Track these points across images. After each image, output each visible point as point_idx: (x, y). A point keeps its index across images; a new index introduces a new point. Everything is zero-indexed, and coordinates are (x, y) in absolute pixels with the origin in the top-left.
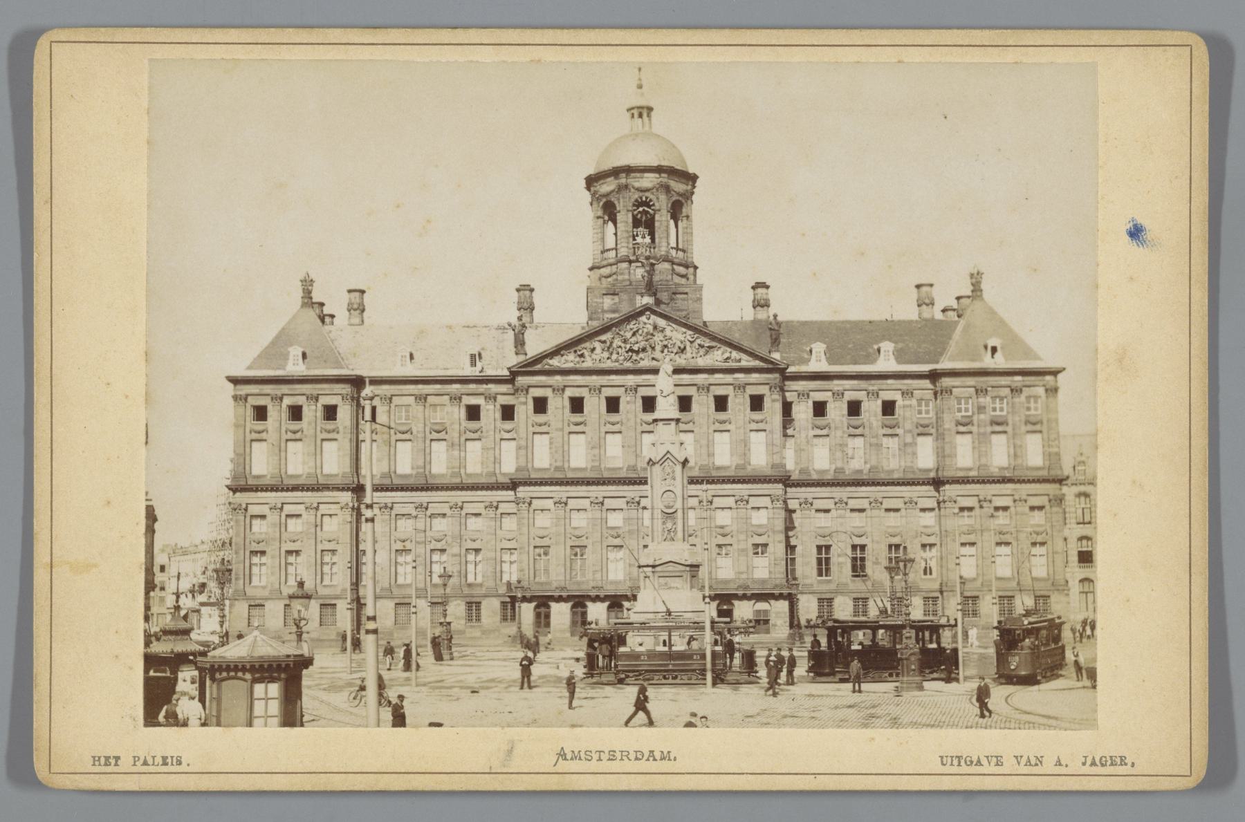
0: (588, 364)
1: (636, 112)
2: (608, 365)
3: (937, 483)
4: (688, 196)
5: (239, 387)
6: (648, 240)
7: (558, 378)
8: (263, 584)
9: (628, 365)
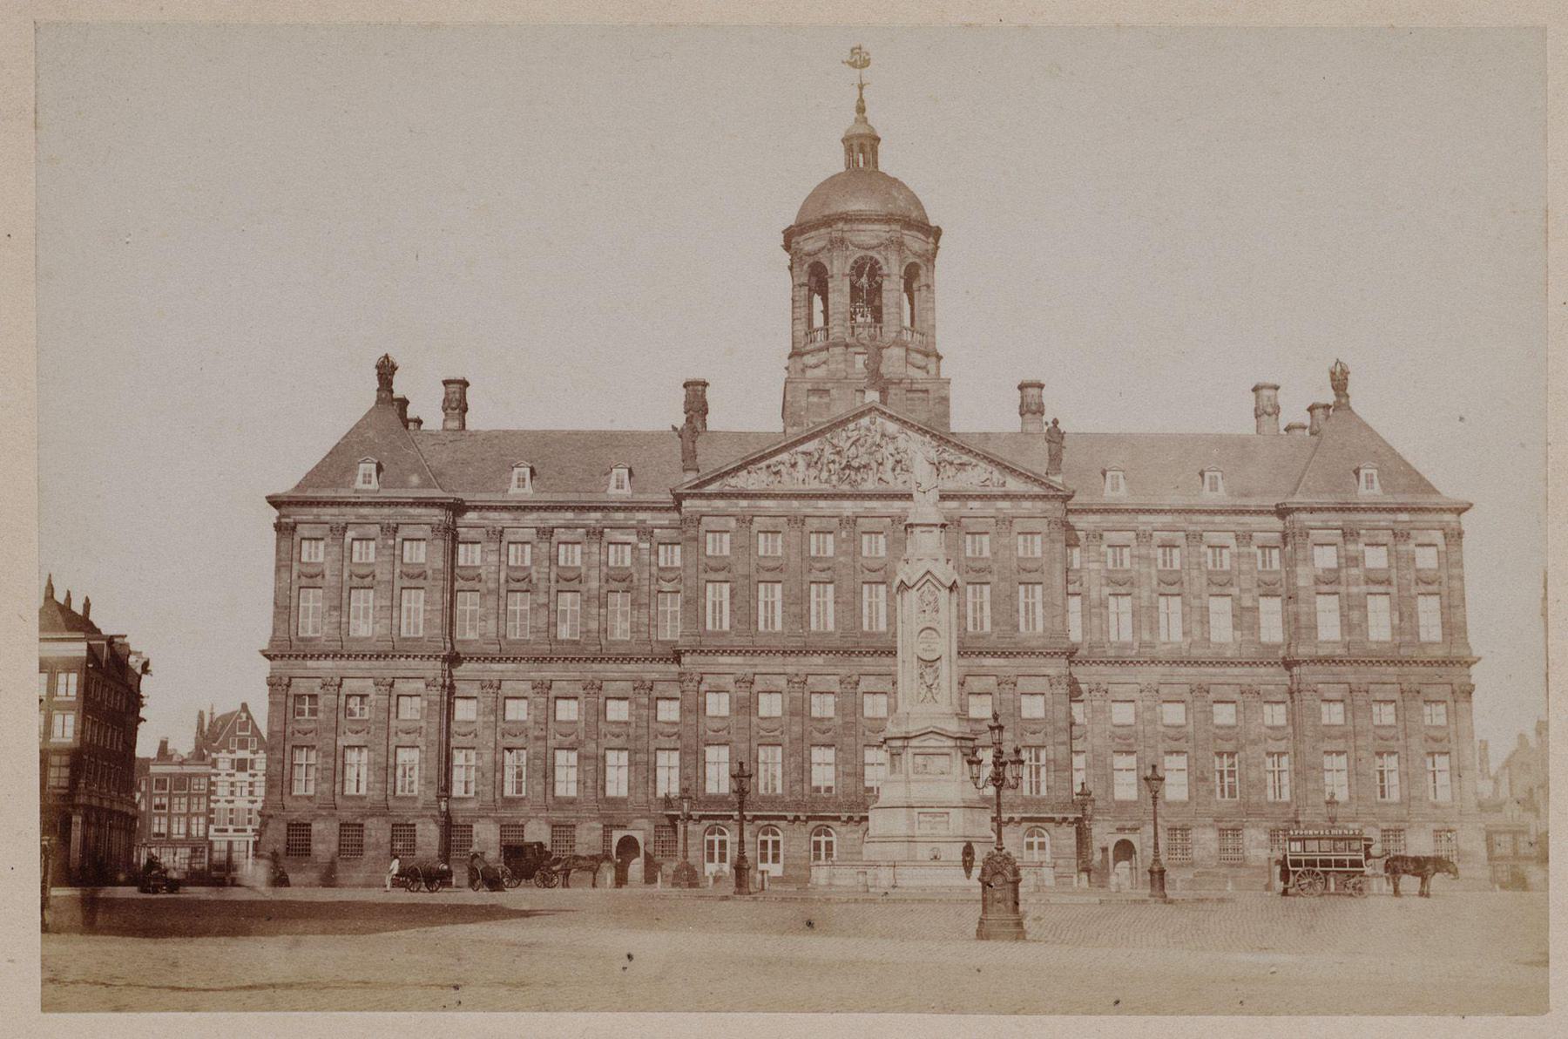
0: (788, 484)
1: (855, 142)
2: (814, 486)
3: (1288, 664)
4: (930, 257)
5: (284, 511)
7: (744, 503)
8: (311, 792)
9: (845, 488)
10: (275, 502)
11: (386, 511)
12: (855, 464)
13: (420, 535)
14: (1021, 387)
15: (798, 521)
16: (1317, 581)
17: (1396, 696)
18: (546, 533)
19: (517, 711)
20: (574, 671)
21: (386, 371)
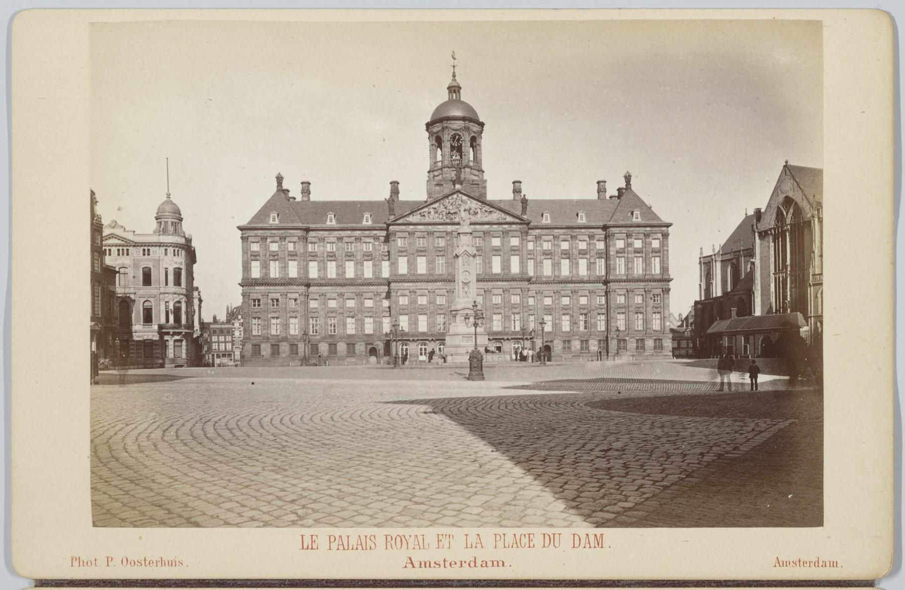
0: (427, 220)
2: (438, 220)
3: (606, 283)
6: (458, 157)
7: (412, 227)
9: (448, 221)
10: (241, 228)
11: (281, 231)
12: (452, 212)
14: (514, 183)
15: (430, 233)
16: (617, 252)
18: (340, 239)
19: (332, 304)
20: (353, 289)
21: (280, 180)
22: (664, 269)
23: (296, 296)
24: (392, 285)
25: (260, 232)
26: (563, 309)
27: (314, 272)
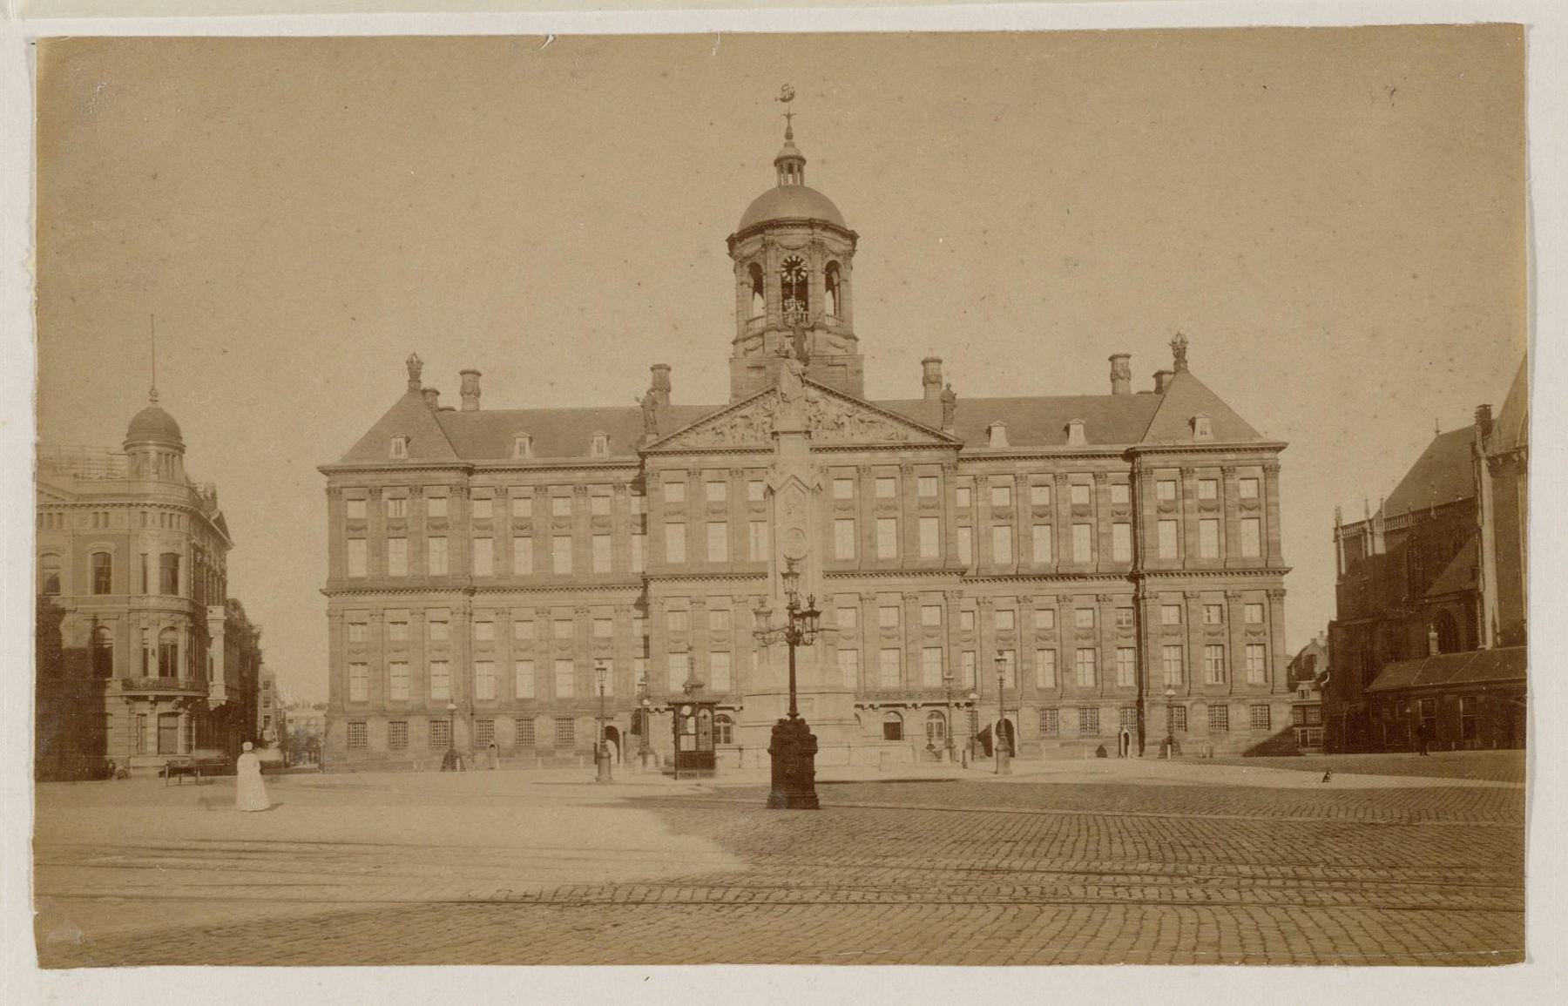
0: (728, 443)
1: (785, 166)
2: (751, 443)
3: (1135, 577)
7: (694, 459)
10: (325, 471)
11: (413, 475)
13: (441, 494)
14: (924, 363)
16: (1160, 510)
17: (1223, 601)
19: (524, 632)
22: (1270, 545)
23: (446, 615)
24: (652, 586)
25: (366, 479)
26: (1038, 638)
27: (484, 564)
